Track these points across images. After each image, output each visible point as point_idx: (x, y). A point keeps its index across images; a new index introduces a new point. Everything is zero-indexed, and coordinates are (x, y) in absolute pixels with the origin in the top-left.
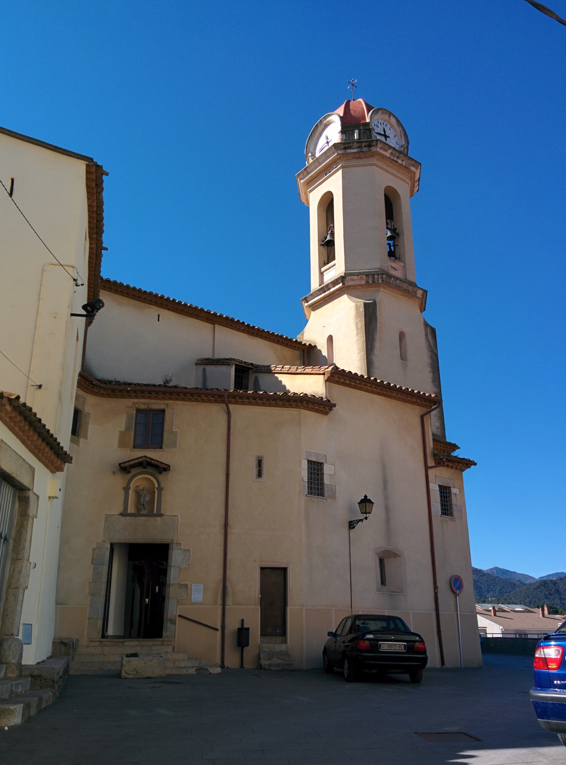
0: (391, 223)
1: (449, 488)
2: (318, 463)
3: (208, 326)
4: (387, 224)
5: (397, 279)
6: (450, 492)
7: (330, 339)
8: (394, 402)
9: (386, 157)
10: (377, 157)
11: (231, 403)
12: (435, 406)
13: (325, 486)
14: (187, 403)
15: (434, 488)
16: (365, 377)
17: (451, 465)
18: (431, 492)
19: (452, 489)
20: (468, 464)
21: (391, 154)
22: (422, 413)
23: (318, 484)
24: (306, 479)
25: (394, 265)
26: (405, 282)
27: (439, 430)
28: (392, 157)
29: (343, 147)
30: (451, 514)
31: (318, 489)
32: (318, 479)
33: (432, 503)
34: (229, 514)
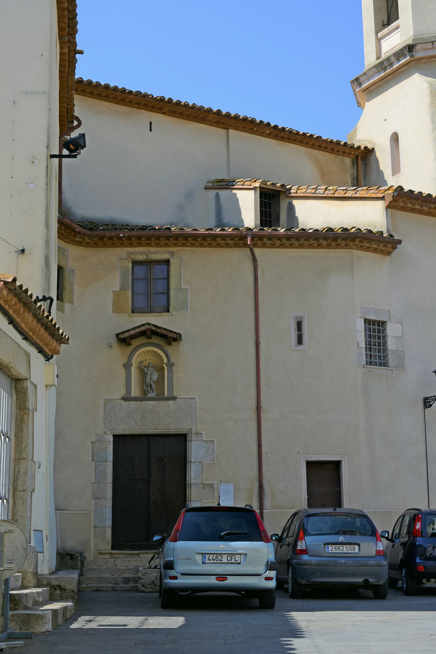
2: (379, 322)
3: (220, 132)
7: (395, 138)
11: (255, 245)
13: (390, 353)
24: (363, 345)
32: (379, 343)
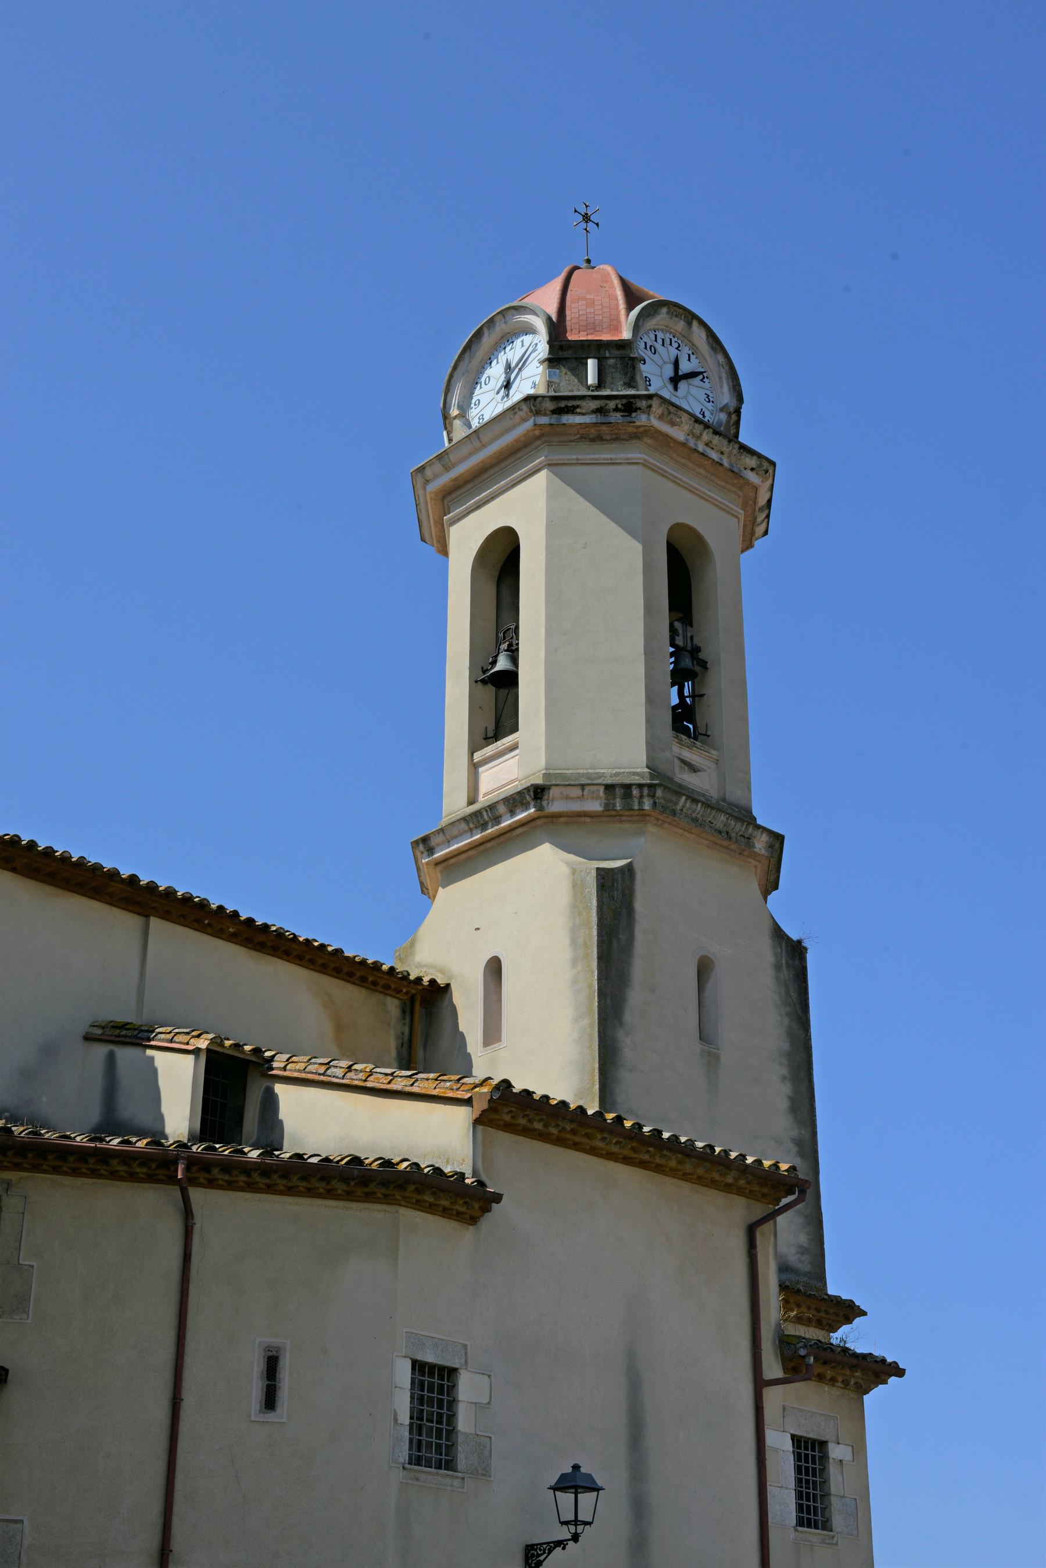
0: (685, 631)
1: (823, 1444)
2: (442, 1369)
3: (126, 922)
4: (673, 631)
5: (694, 798)
6: (824, 1457)
7: (494, 968)
8: (670, 1185)
9: (676, 441)
10: (649, 441)
11: (193, 1181)
12: (791, 1198)
13: (461, 1439)
14: (68, 1181)
15: (780, 1442)
16: (590, 1112)
17: (829, 1374)
18: (770, 1456)
19: (831, 1446)
20: (880, 1370)
21: (691, 433)
22: (754, 1219)
23: (439, 1432)
24: (405, 1418)
25: (687, 754)
26: (719, 810)
27: (806, 1258)
28: (692, 443)
29: (550, 406)
30: (826, 1525)
31: (439, 1446)
32: (440, 1416)
33: (771, 1491)
34: (175, 1519)
